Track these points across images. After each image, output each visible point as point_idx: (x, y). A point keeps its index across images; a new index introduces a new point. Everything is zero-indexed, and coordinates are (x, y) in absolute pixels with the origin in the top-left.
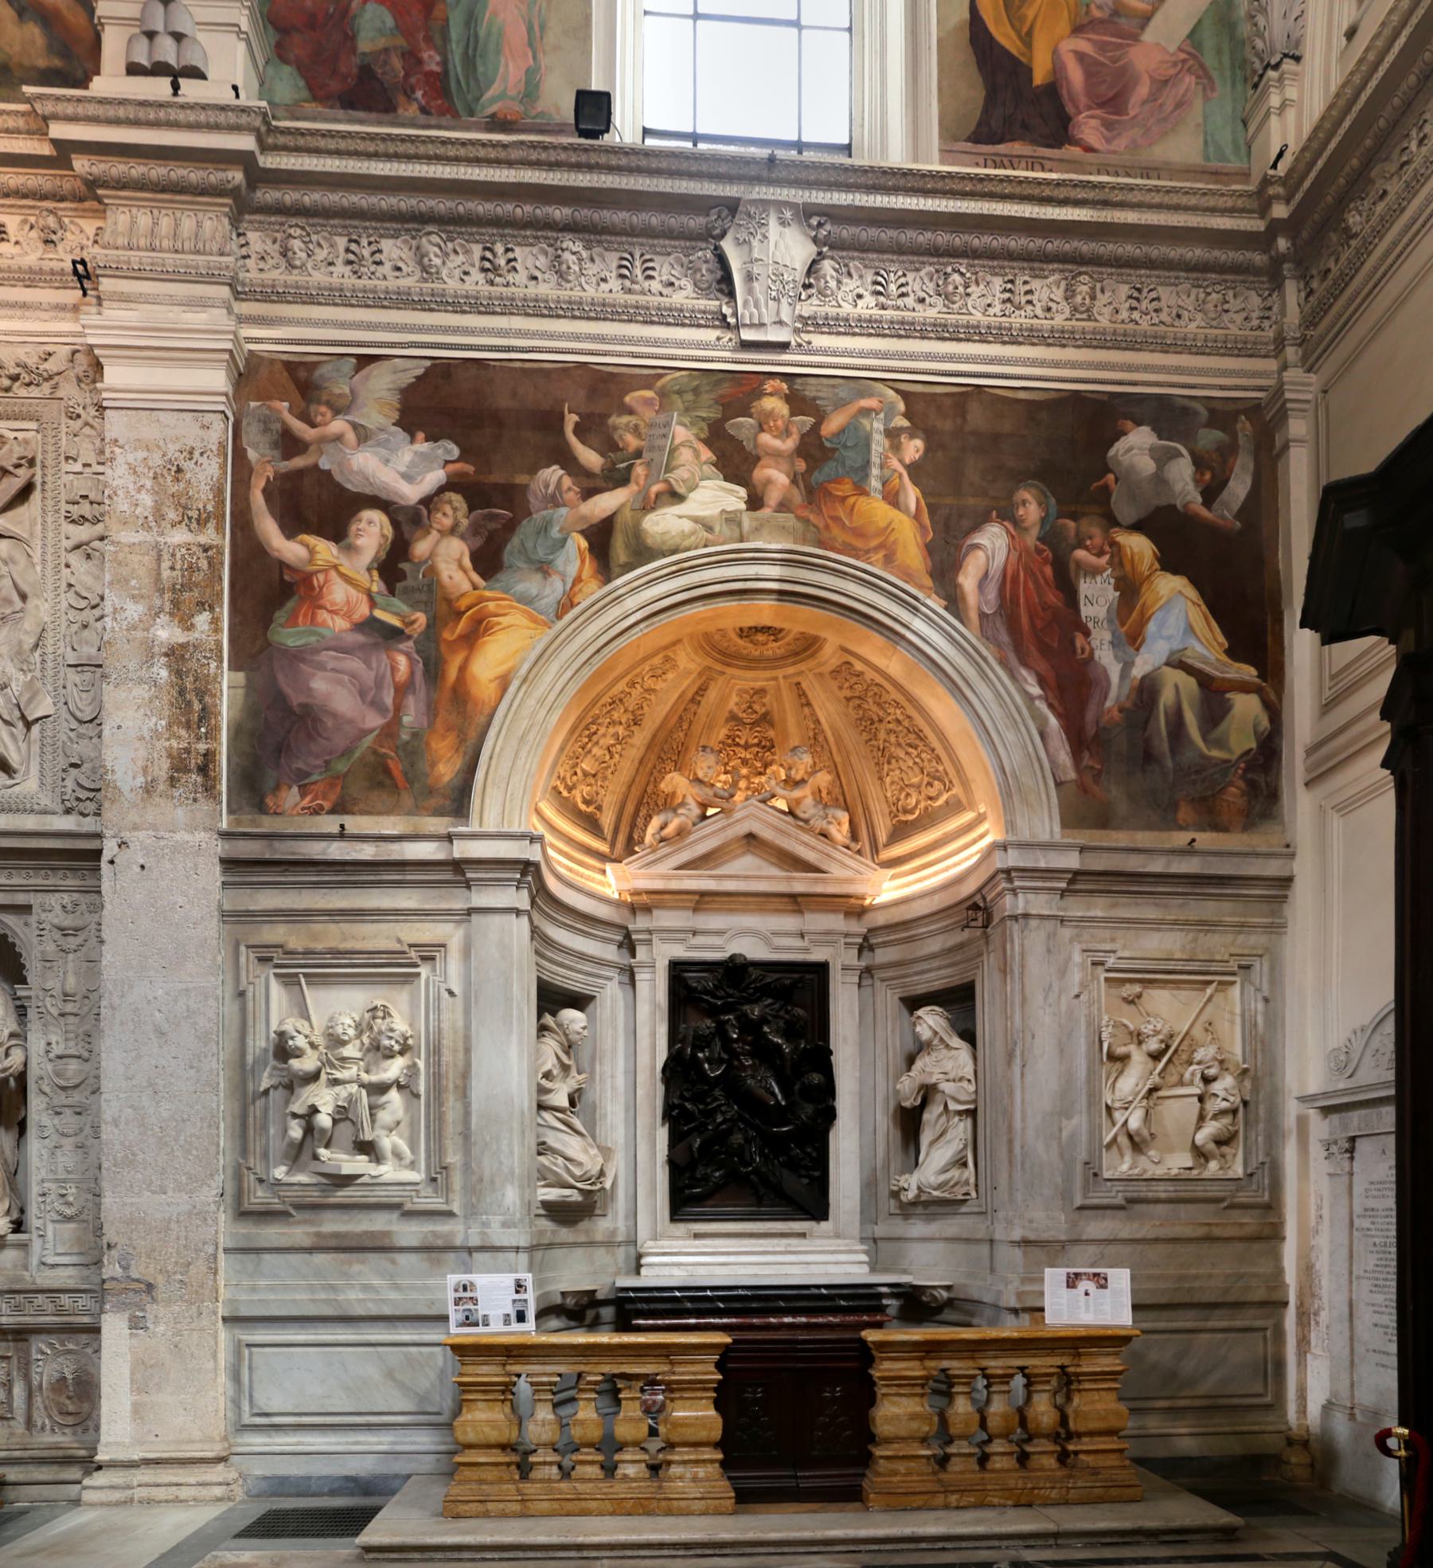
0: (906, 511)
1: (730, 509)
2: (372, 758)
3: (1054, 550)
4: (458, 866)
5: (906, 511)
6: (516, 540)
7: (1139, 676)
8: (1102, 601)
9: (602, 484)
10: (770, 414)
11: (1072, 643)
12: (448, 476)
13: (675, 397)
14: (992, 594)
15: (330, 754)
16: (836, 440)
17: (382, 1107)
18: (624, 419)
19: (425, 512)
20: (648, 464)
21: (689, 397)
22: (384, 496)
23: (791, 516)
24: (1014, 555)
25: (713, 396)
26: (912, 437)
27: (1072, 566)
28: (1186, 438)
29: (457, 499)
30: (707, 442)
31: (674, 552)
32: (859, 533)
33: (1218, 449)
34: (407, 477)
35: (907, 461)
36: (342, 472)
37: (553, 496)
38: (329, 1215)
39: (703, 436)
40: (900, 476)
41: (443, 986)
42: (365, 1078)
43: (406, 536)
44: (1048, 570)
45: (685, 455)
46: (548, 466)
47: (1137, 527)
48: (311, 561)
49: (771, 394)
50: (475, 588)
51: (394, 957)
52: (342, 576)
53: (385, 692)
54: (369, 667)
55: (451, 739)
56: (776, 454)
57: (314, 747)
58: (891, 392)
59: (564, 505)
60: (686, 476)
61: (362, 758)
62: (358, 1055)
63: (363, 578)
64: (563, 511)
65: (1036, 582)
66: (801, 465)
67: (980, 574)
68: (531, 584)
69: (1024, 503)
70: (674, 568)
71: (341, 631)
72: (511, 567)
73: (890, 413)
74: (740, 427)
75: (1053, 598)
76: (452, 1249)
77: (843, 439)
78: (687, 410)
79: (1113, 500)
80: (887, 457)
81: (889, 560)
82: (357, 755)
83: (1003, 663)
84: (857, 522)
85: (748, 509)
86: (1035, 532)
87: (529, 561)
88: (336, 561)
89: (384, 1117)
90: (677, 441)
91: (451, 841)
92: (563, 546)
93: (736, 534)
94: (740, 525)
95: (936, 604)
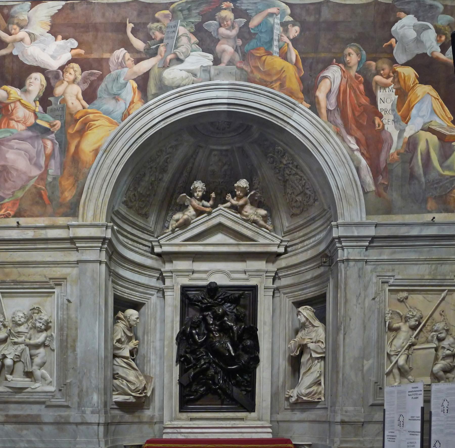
0: (291, 62)
1: (204, 65)
2: (34, 190)
3: (364, 76)
4: (72, 240)
5: (291, 62)
6: (103, 85)
7: (408, 137)
8: (389, 101)
9: (144, 56)
10: (224, 19)
11: (374, 122)
12: (72, 56)
13: (179, 14)
14: (333, 99)
15: (15, 188)
16: (256, 29)
17: (36, 355)
18: (156, 25)
19: (61, 73)
20: (166, 45)
21: (186, 12)
22: (42, 66)
23: (235, 67)
24: (344, 81)
25: (197, 11)
26: (294, 25)
27: (374, 84)
28: (433, 19)
29: (76, 66)
30: (193, 33)
31: (178, 87)
32: (268, 74)
33: (449, 25)
34: (53, 57)
35: (291, 37)
36: (23, 56)
37: (121, 63)
38: (12, 406)
39: (192, 31)
40: (288, 44)
41: (65, 298)
42: (27, 341)
43: (52, 84)
44: (362, 87)
45: (184, 40)
46: (119, 49)
47: (407, 64)
48: (8, 98)
49: (225, 9)
50: (84, 108)
51: (43, 284)
52: (23, 104)
53: (41, 159)
54: (33, 146)
55: (71, 180)
56: (228, 38)
57: (8, 185)
58: (284, 5)
59: (126, 67)
60: (184, 50)
61: (29, 190)
62: (26, 331)
63: (32, 105)
64: (126, 70)
65: (355, 93)
66: (240, 42)
67: (327, 91)
68: (110, 105)
69: (349, 54)
70: (177, 95)
71: (21, 130)
72: (100, 98)
73: (283, 14)
74: (211, 25)
75: (364, 100)
76: (69, 423)
77: (260, 28)
78: (185, 19)
79: (394, 51)
80: (282, 36)
81: (282, 87)
82: (27, 188)
83: (338, 134)
84: (267, 68)
85: (213, 65)
86: (355, 68)
87: (109, 94)
88: (20, 98)
89: (37, 360)
90: (180, 34)
91: (69, 229)
92: (125, 87)
93: (208, 77)
94: (209, 72)
95: (305, 106)
